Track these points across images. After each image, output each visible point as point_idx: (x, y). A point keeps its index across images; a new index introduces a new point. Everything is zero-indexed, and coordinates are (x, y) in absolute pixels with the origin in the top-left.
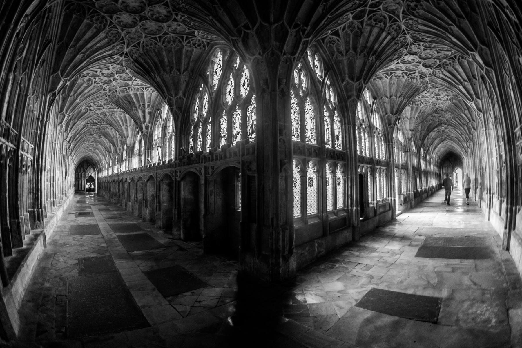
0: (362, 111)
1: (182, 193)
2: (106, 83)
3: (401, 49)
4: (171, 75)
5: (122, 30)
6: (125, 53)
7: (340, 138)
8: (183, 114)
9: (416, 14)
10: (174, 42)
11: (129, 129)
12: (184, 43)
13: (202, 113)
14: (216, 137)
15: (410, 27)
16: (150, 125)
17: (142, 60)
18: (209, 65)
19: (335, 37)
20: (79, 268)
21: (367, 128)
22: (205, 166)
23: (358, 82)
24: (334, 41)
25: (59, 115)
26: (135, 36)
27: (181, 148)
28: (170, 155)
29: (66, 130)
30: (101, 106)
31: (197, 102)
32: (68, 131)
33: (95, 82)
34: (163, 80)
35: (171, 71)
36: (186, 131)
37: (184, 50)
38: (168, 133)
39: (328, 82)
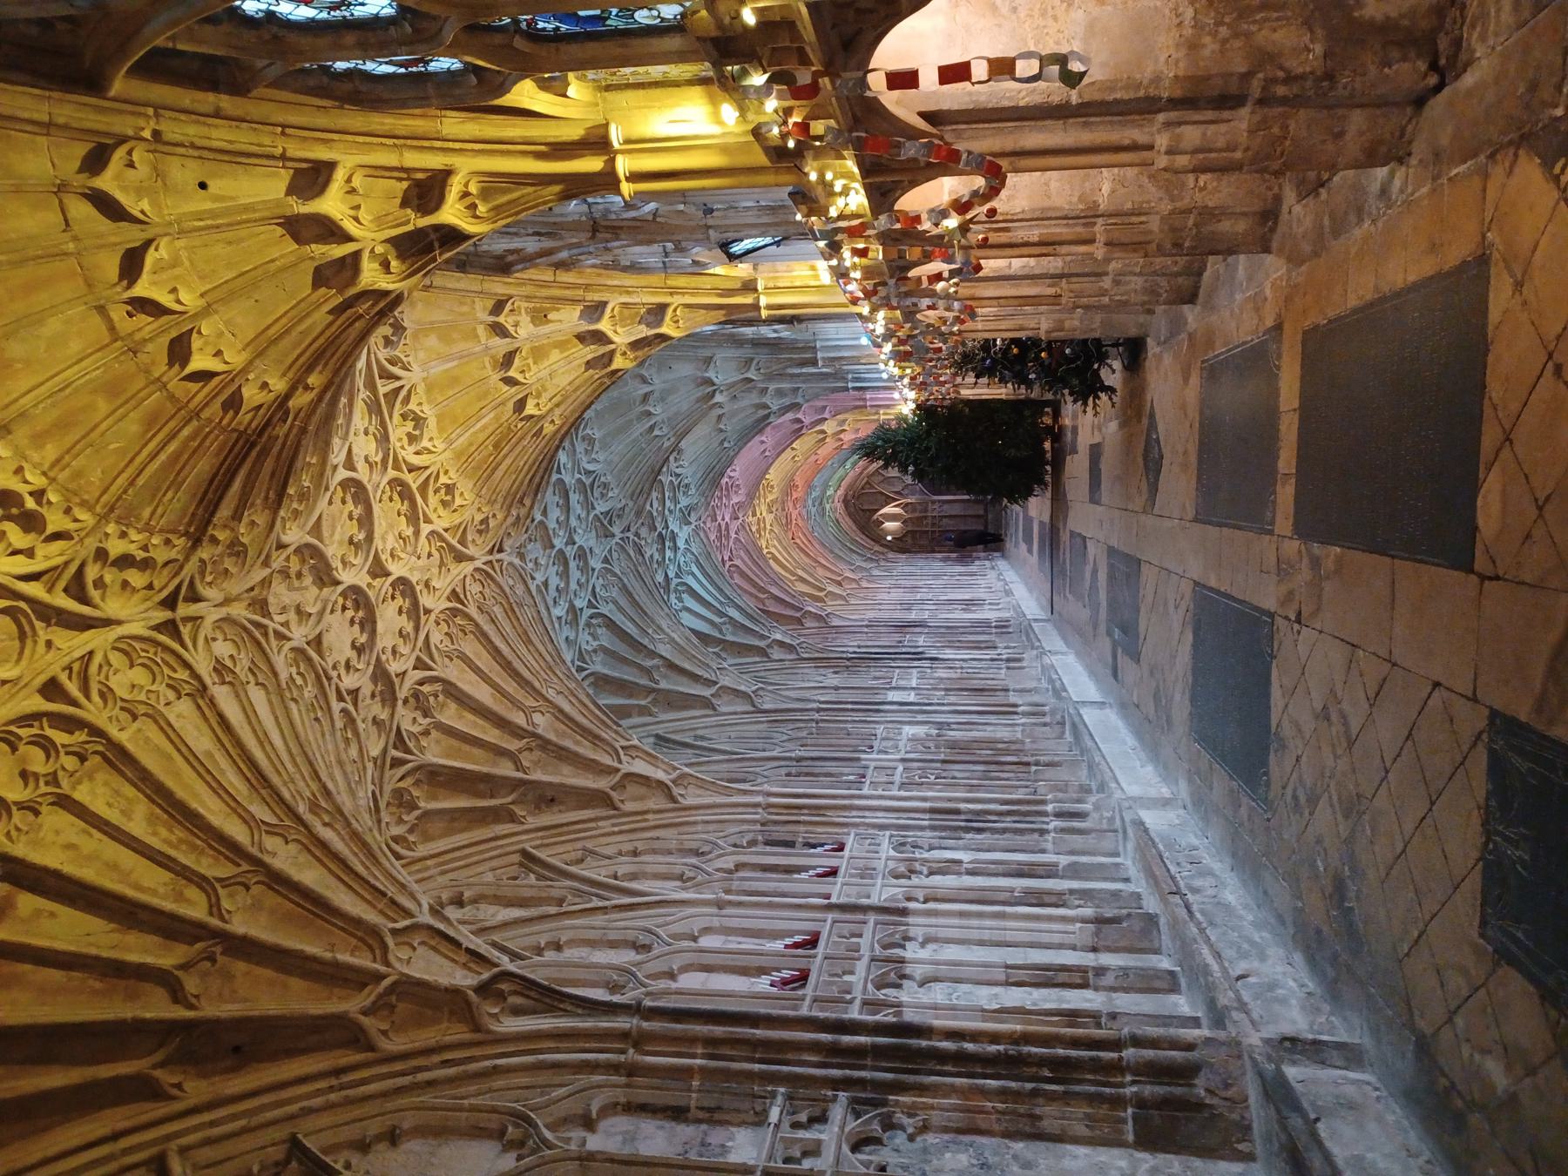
2: (415, 603)
25: (629, 806)
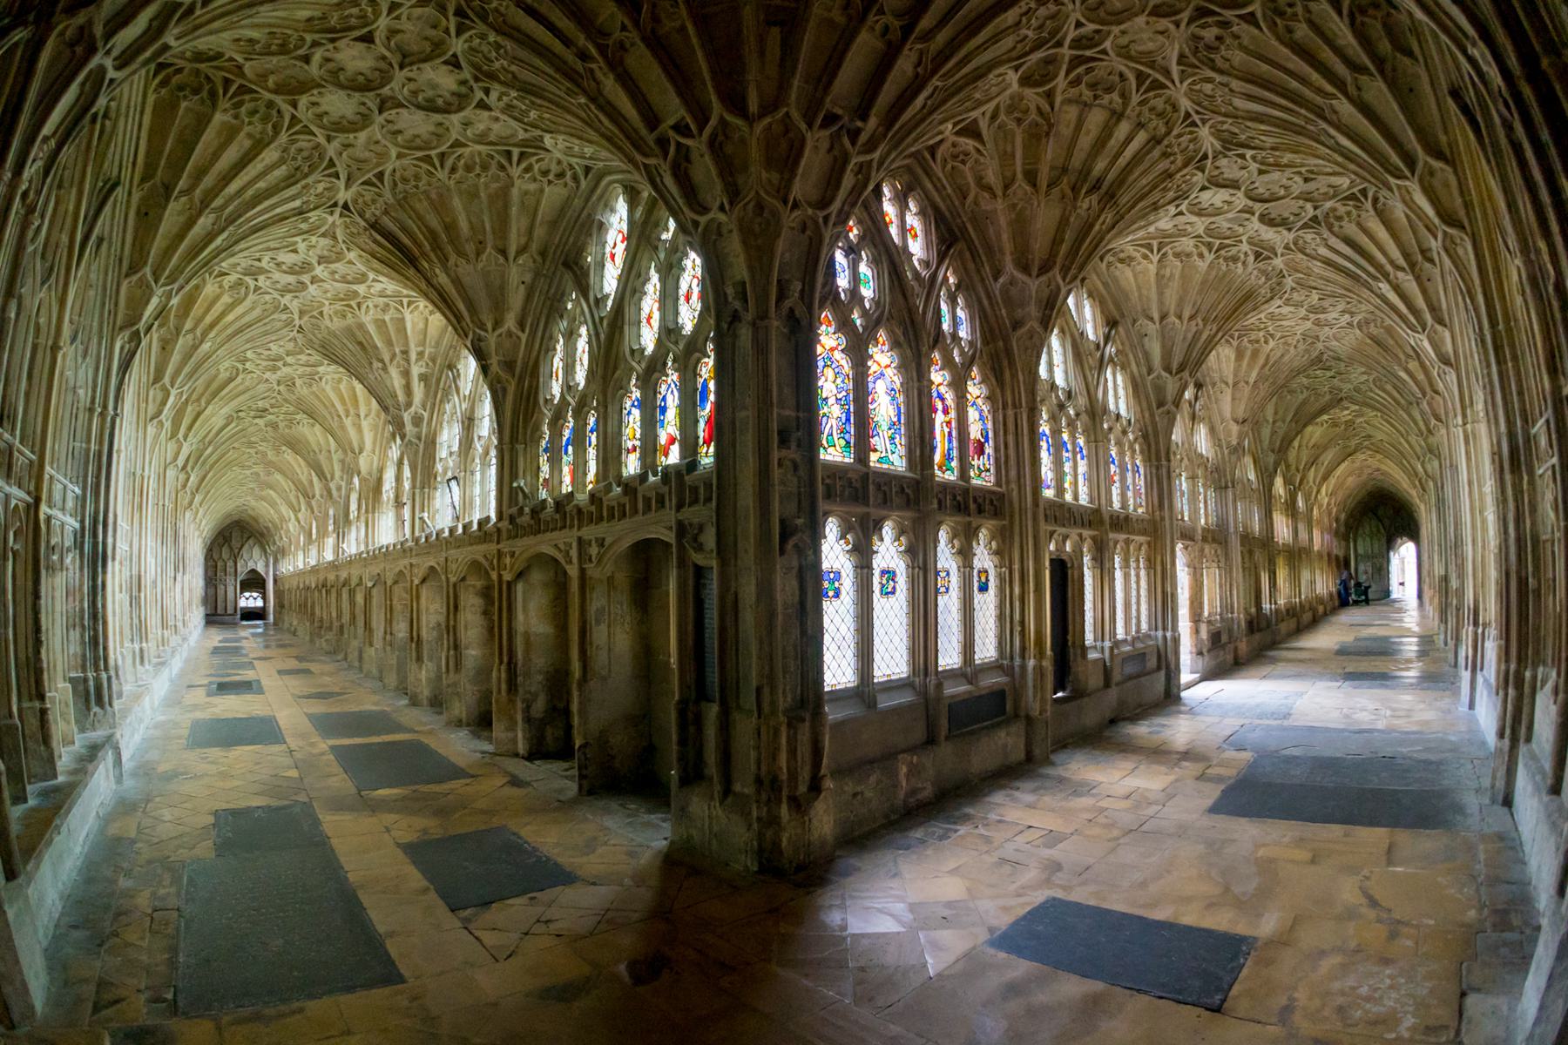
0: (1065, 362)
1: (520, 617)
2: (290, 291)
3: (1185, 171)
4: (480, 265)
5: (329, 139)
6: (341, 203)
7: (989, 449)
8: (521, 380)
9: (1219, 63)
10: (485, 168)
11: (366, 425)
12: (515, 171)
13: (574, 379)
14: (611, 454)
15: (1206, 105)
16: (426, 415)
17: (391, 224)
18: (591, 235)
19: (969, 144)
20: (219, 836)
21: (1084, 417)
22: (580, 539)
23: (1044, 278)
24: (967, 154)
26: (367, 154)
27: (515, 485)
28: (484, 504)
29: (174, 435)
30: (278, 358)
31: (559, 347)
32: (180, 435)
33: (257, 288)
34: (457, 282)
35: (478, 254)
36: (529, 432)
37: (515, 192)
38: (479, 437)
39: (951, 280)
